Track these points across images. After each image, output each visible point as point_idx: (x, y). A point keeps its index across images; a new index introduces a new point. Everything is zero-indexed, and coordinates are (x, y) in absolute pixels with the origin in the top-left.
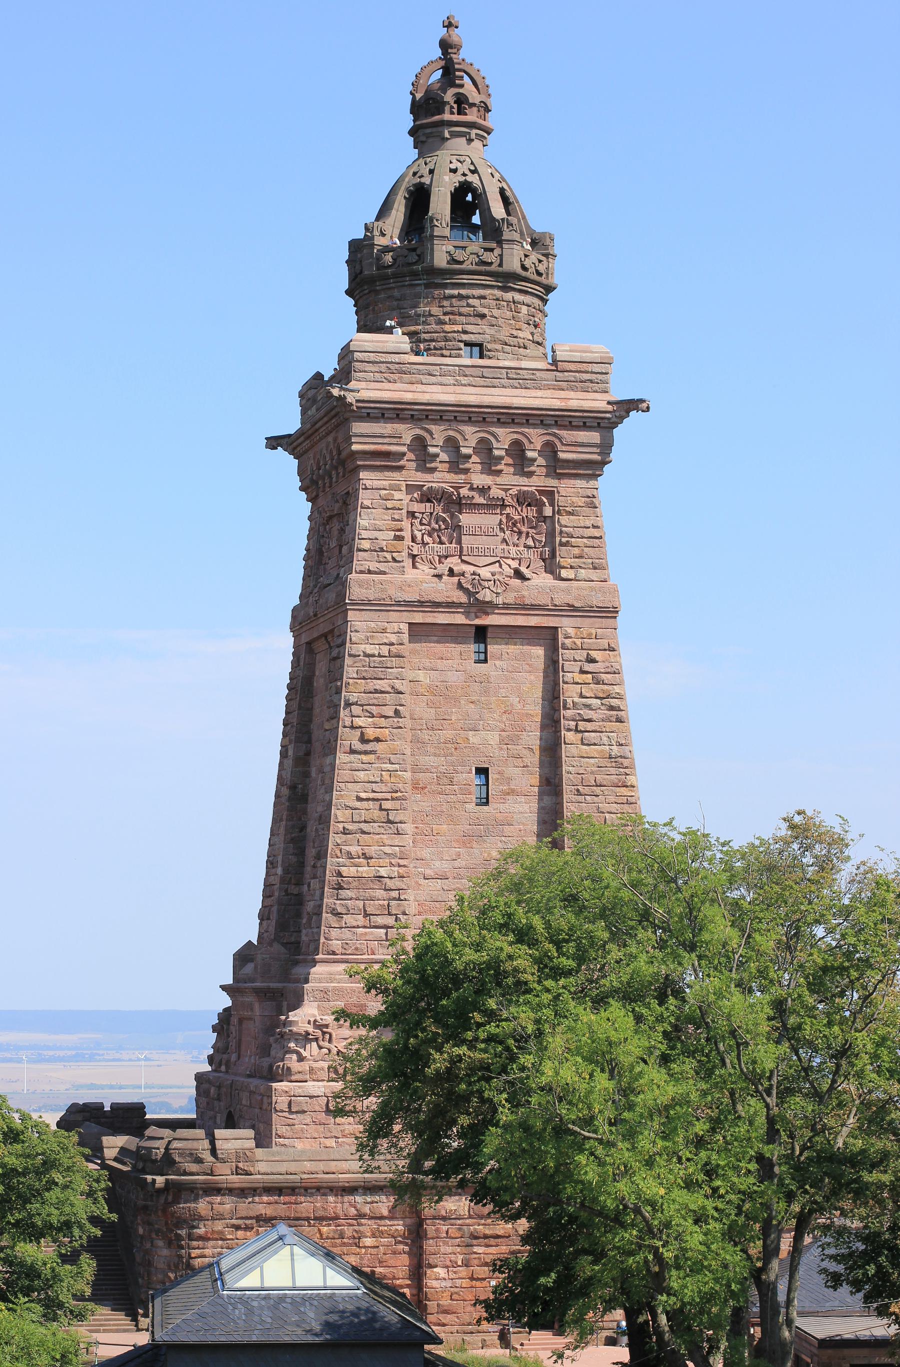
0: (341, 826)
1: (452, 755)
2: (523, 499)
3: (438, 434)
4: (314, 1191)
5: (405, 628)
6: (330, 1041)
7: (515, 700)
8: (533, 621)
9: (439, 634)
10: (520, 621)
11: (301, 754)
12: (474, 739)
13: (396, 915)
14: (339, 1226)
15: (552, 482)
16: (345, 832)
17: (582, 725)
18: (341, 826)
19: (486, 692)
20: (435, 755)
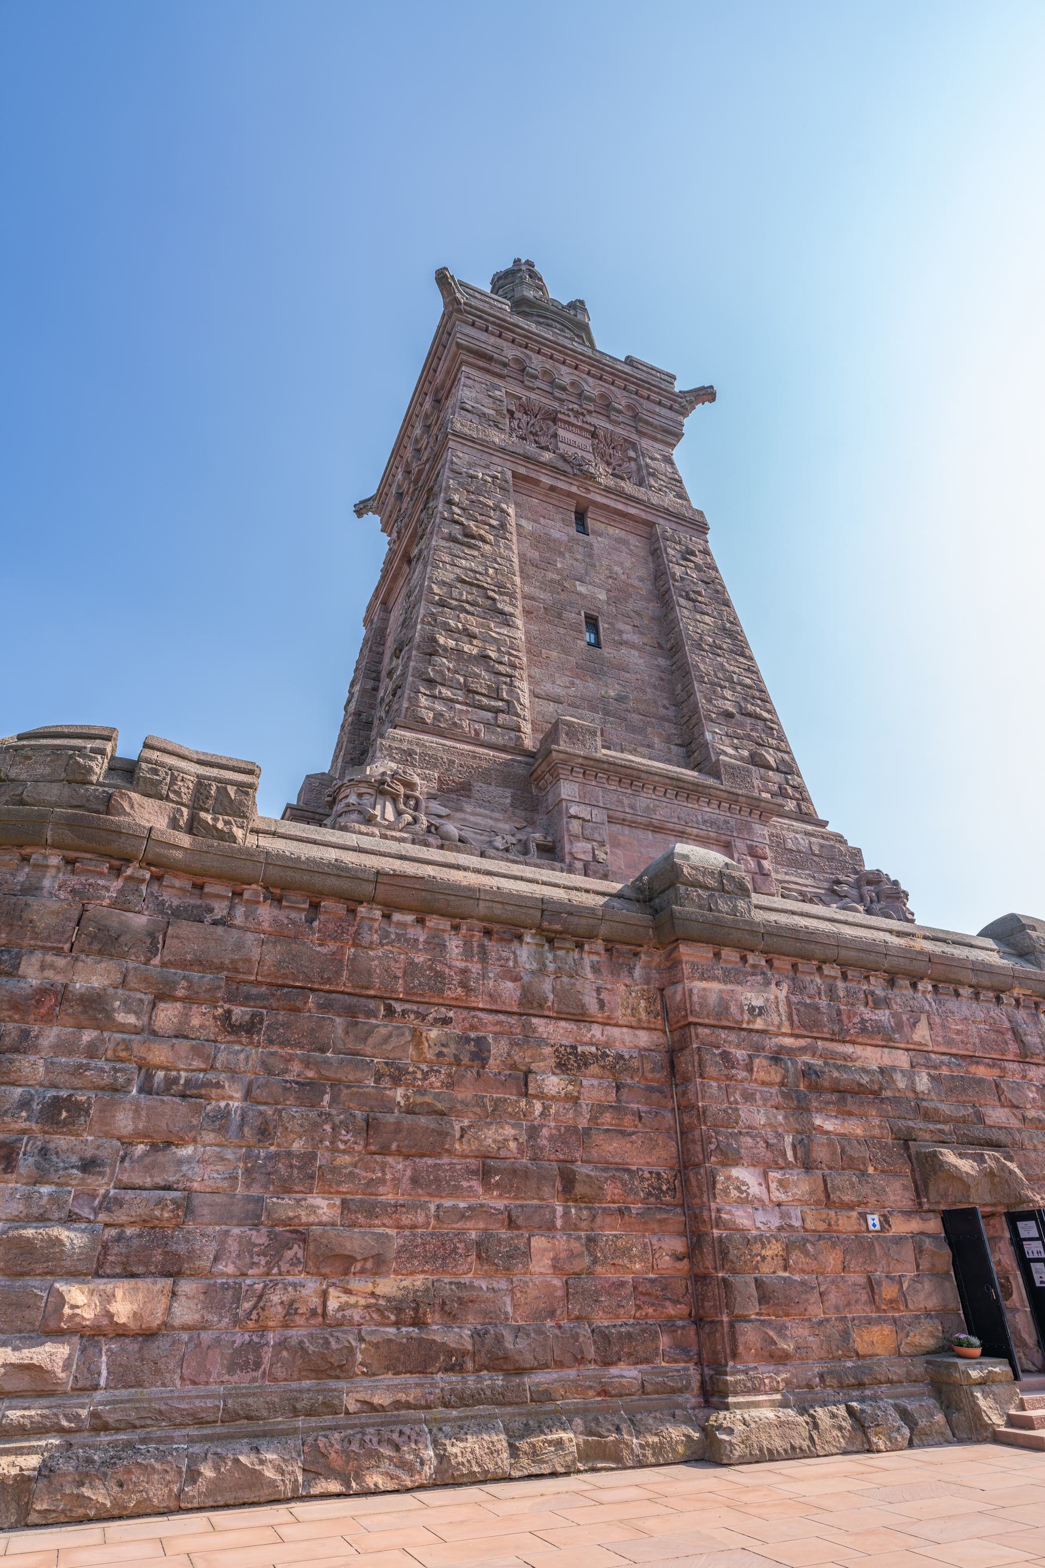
0: (437, 598)
1: (558, 593)
2: (611, 441)
3: (537, 363)
4: (410, 918)
5: (509, 475)
6: (416, 808)
7: (616, 569)
8: (632, 511)
9: (541, 497)
10: (620, 507)
11: (369, 687)
12: (581, 588)
13: (507, 701)
14: (473, 1028)
15: (634, 437)
16: (442, 604)
17: (692, 595)
18: (437, 598)
19: (591, 556)
20: (541, 588)
